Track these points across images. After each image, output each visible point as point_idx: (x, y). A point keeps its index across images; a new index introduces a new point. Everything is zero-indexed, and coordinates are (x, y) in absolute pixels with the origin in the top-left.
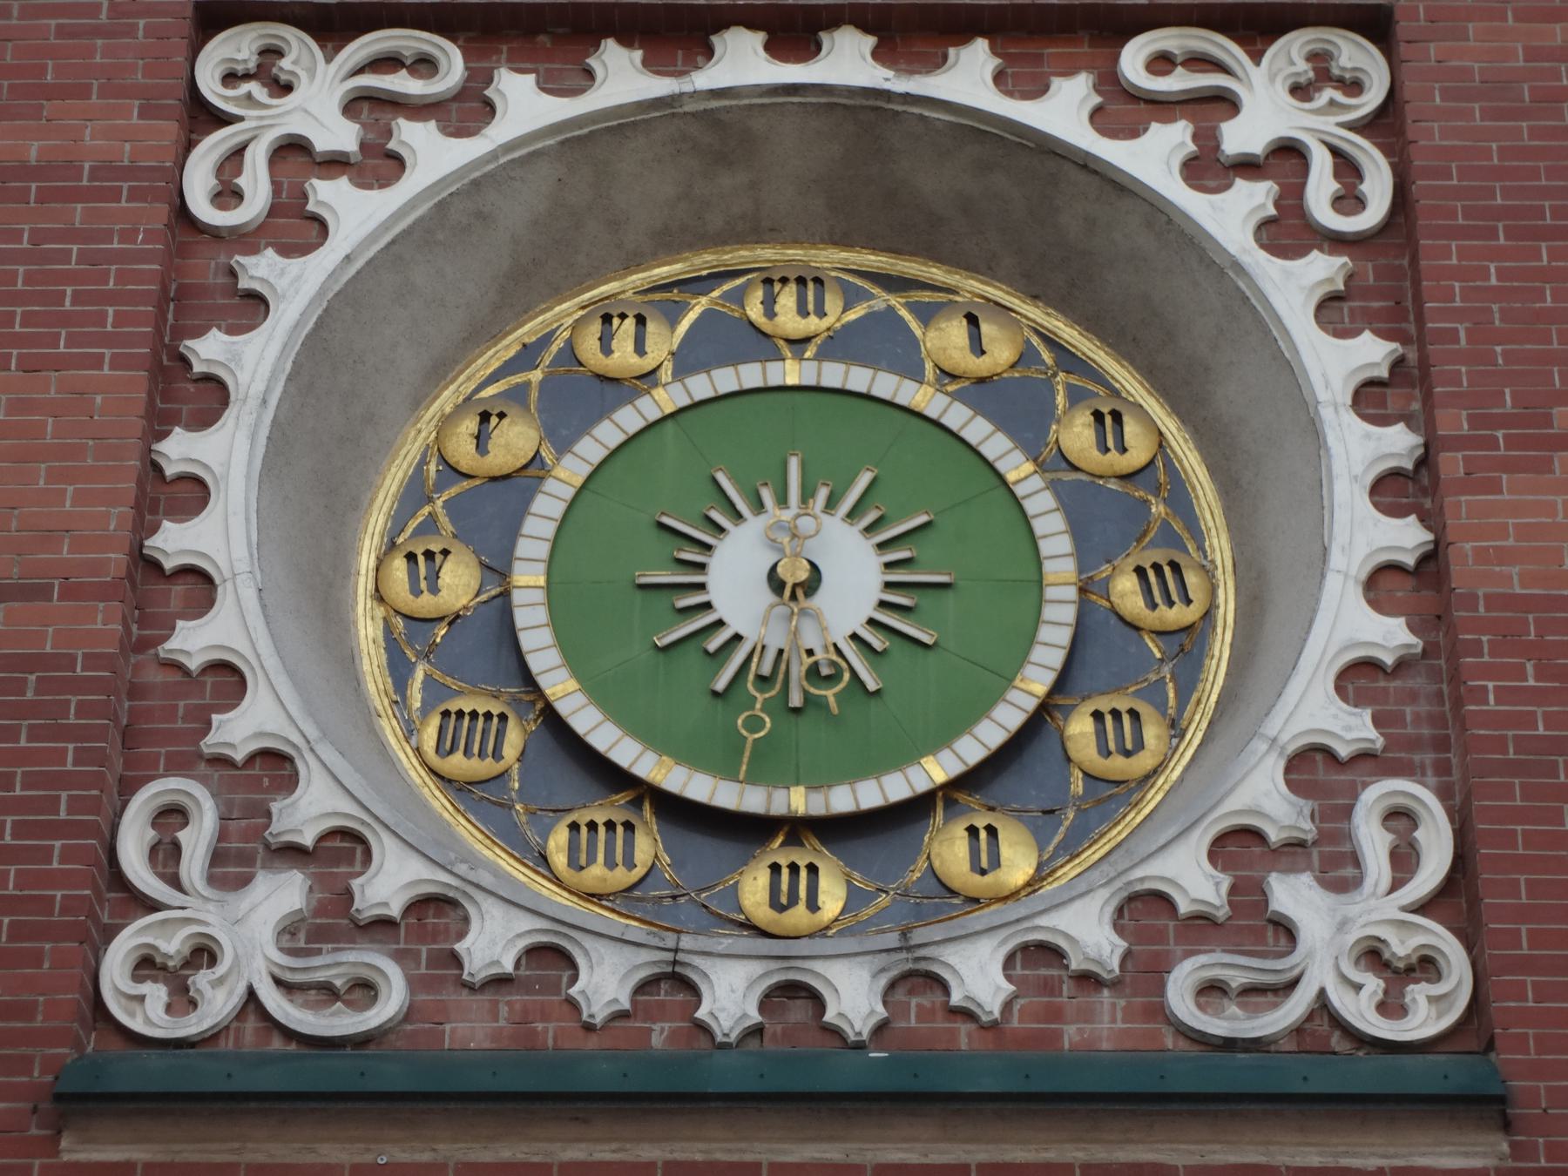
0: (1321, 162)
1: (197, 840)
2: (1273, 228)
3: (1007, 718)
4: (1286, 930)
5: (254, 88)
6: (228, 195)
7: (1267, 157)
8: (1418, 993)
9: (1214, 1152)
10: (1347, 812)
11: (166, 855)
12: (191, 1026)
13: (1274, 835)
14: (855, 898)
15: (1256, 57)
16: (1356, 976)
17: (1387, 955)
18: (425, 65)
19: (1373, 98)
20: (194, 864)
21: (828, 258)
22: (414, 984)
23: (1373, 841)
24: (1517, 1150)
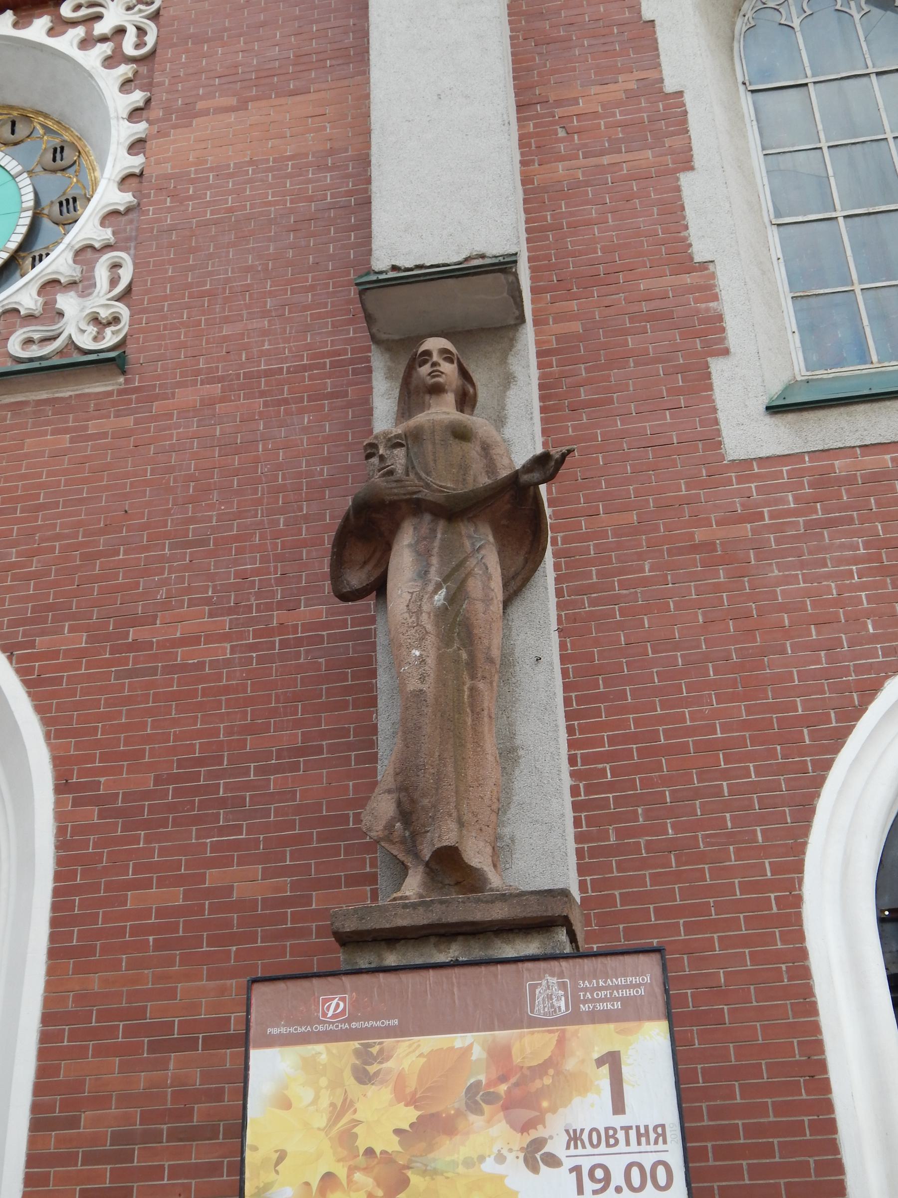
2: (110, 60)
4: (61, 314)
7: (112, 35)
8: (108, 331)
9: (5, 399)
13: (63, 280)
16: (84, 326)
17: (99, 319)
23: (102, 274)
24: (127, 381)
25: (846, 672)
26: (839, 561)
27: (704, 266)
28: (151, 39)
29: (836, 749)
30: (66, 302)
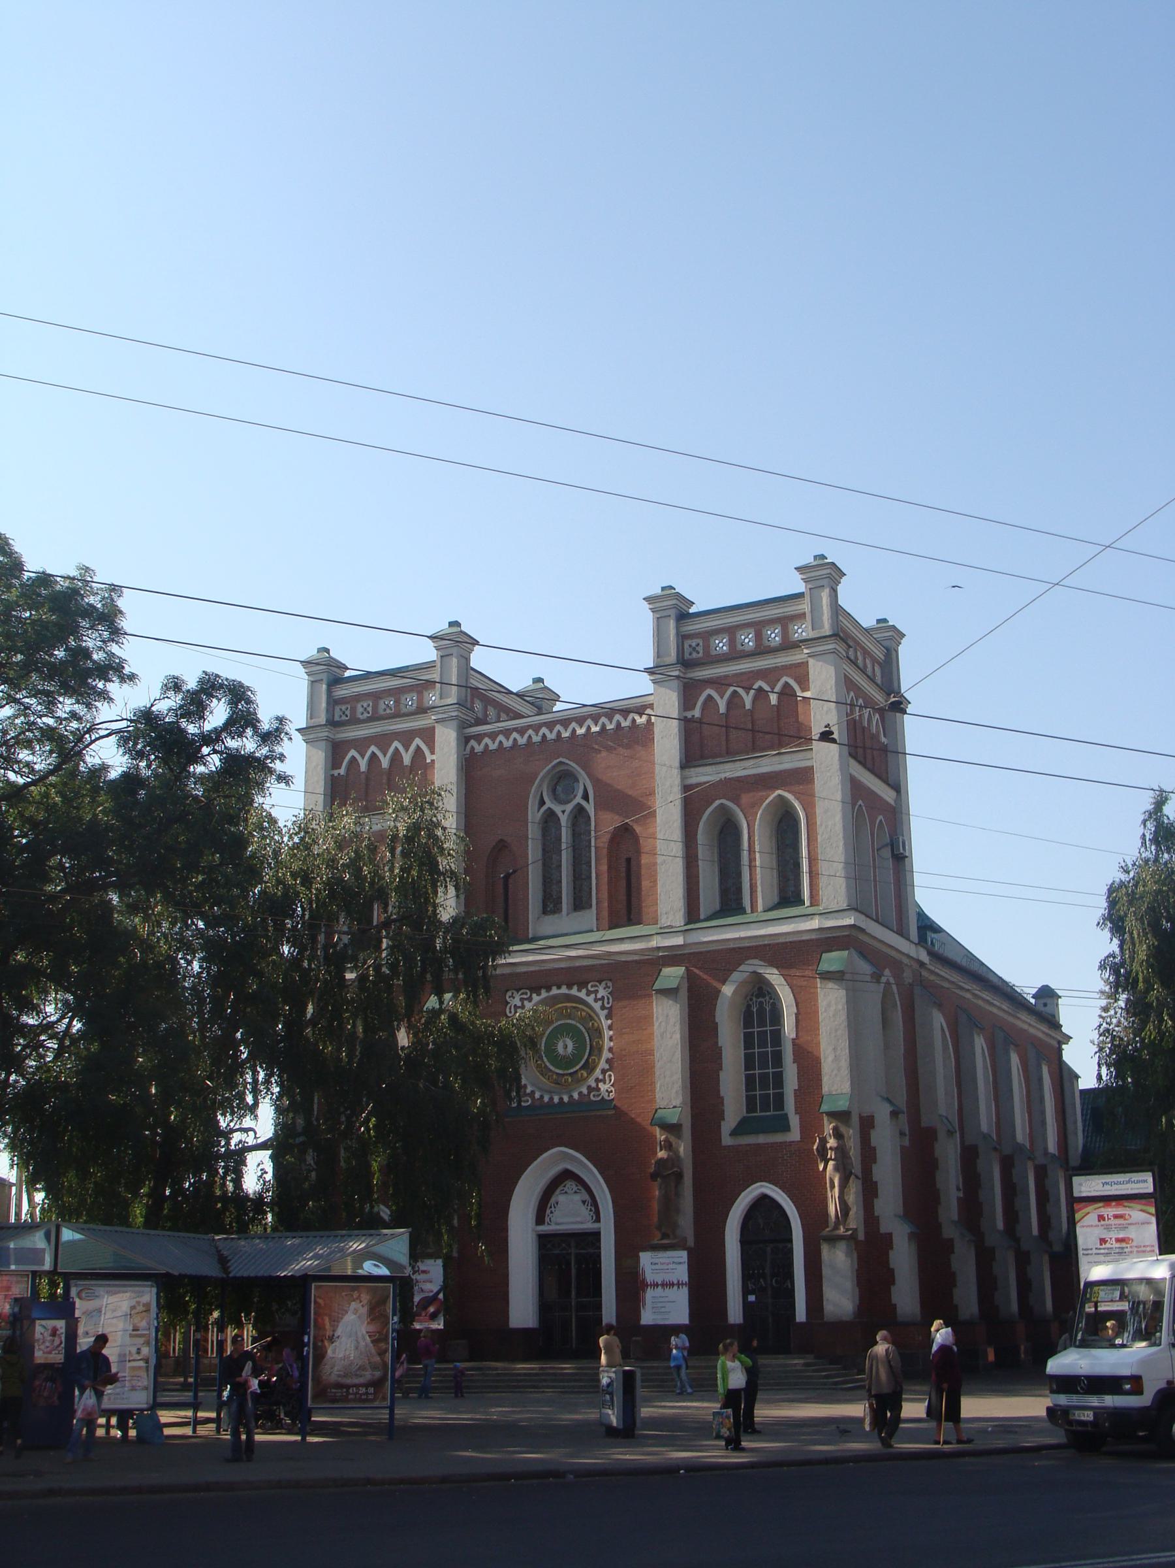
0: (606, 998)
18: (526, 994)
19: (610, 990)
21: (568, 1005)
28: (611, 1001)
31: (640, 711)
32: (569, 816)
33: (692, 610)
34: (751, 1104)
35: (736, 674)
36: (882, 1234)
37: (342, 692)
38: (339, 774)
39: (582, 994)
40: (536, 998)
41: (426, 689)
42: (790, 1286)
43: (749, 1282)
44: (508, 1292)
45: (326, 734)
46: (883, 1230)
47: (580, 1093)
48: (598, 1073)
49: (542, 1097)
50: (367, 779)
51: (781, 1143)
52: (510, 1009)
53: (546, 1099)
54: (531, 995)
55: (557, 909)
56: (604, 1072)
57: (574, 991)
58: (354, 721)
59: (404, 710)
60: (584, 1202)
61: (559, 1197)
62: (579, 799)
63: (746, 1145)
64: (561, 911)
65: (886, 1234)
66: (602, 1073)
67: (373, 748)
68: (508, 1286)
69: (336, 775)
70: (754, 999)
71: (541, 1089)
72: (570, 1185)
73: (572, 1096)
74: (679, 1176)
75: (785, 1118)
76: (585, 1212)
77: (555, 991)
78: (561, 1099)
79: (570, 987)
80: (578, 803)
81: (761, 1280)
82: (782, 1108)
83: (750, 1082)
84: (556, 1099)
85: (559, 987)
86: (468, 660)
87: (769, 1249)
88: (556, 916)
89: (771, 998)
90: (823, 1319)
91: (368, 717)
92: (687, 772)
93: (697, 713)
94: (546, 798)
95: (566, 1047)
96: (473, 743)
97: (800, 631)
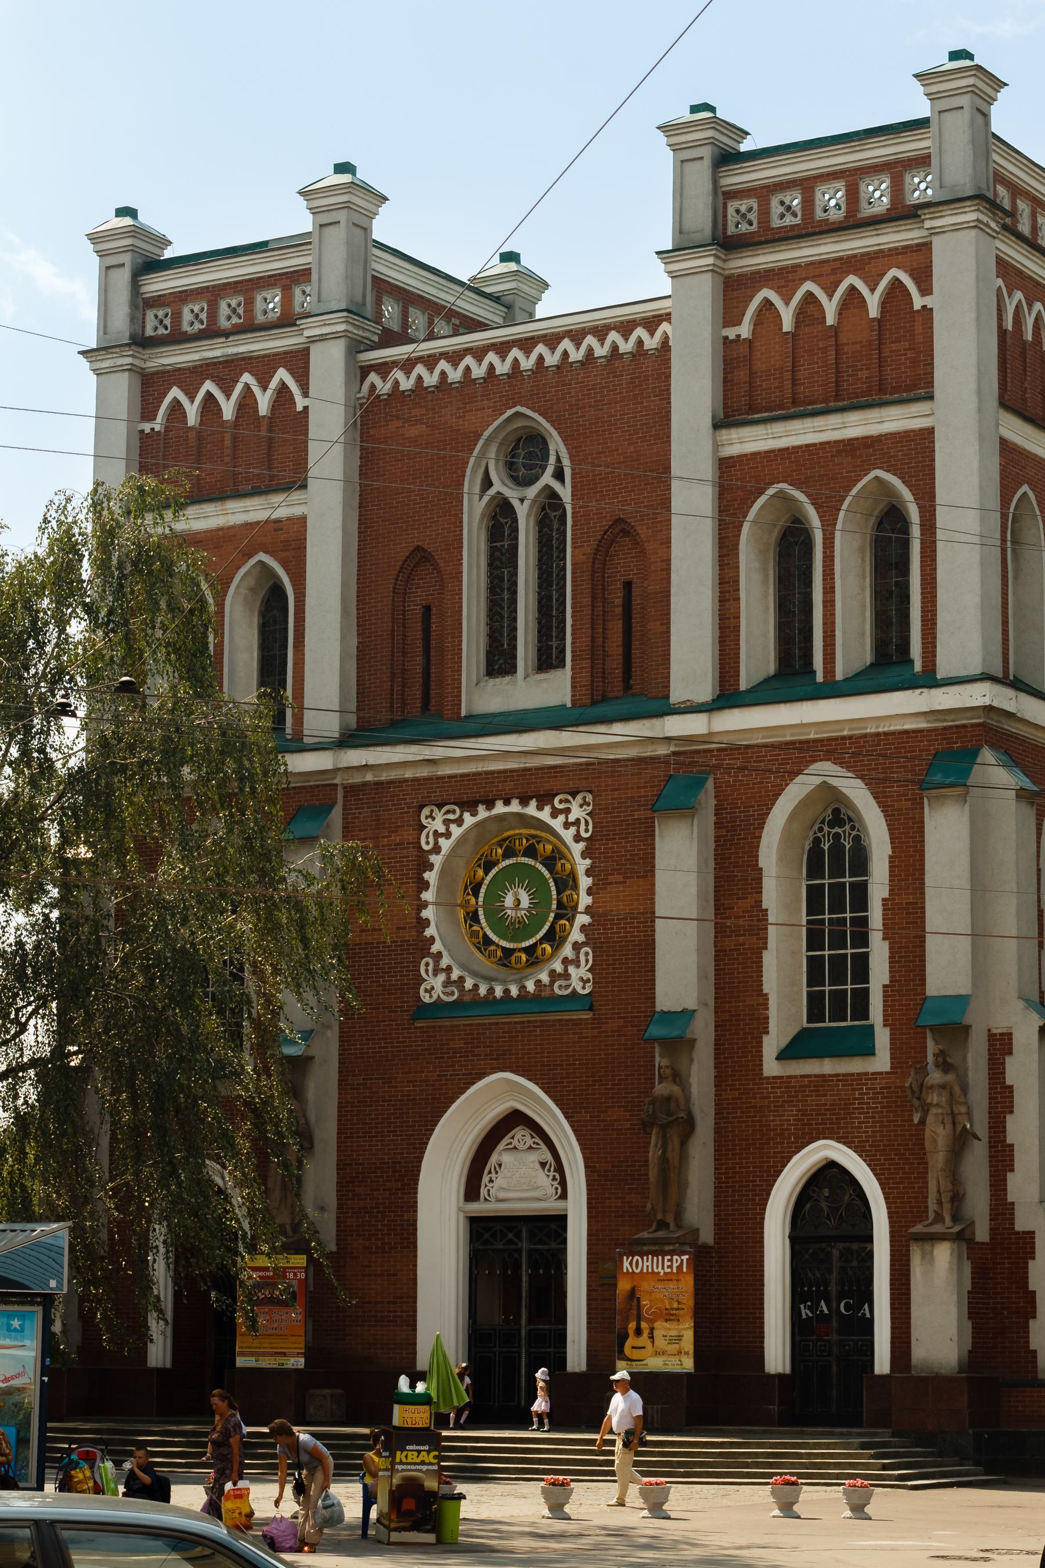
1: (430, 968)
3: (546, 927)
5: (429, 820)
6: (428, 843)
8: (587, 985)
10: (579, 953)
11: (427, 971)
12: (432, 1001)
14: (527, 961)
15: (574, 798)
18: (454, 812)
19: (591, 807)
20: (430, 972)
22: (459, 991)
25: (783, 1152)
26: (788, 1115)
27: (766, 995)
29: (778, 1176)
30: (572, 970)
31: (652, 323)
32: (531, 506)
33: (745, 146)
34: (815, 1007)
35: (812, 263)
36: (1018, 1233)
37: (158, 284)
38: (152, 429)
39: (545, 815)
40: (469, 820)
41: (297, 282)
42: (868, 1315)
43: (802, 1306)
44: (415, 1311)
45: (129, 360)
46: (1019, 1226)
47: (538, 982)
48: (567, 951)
49: (476, 987)
50: (200, 438)
51: (858, 1074)
52: (427, 836)
53: (483, 991)
54: (461, 815)
55: (510, 669)
56: (577, 947)
57: (531, 810)
58: (178, 338)
59: (260, 319)
60: (543, 1165)
61: (500, 1155)
62: (547, 478)
63: (802, 1076)
64: (515, 672)
65: (1024, 1233)
66: (573, 949)
67: (209, 386)
68: (415, 1302)
69: (148, 431)
70: (826, 828)
71: (474, 974)
72: (521, 1135)
73: (525, 987)
74: (689, 1125)
75: (869, 1031)
76: (545, 1182)
77: (500, 808)
78: (507, 991)
79: (524, 802)
80: (547, 487)
81: (823, 1303)
82: (866, 1017)
83: (815, 973)
84: (499, 992)
85: (507, 802)
86: (367, 230)
87: (835, 1253)
88: (507, 679)
89: (853, 828)
90: (909, 1371)
91: (200, 330)
92: (725, 435)
93: (745, 330)
94: (494, 477)
95: (518, 902)
96: (373, 377)
97: (923, 186)
